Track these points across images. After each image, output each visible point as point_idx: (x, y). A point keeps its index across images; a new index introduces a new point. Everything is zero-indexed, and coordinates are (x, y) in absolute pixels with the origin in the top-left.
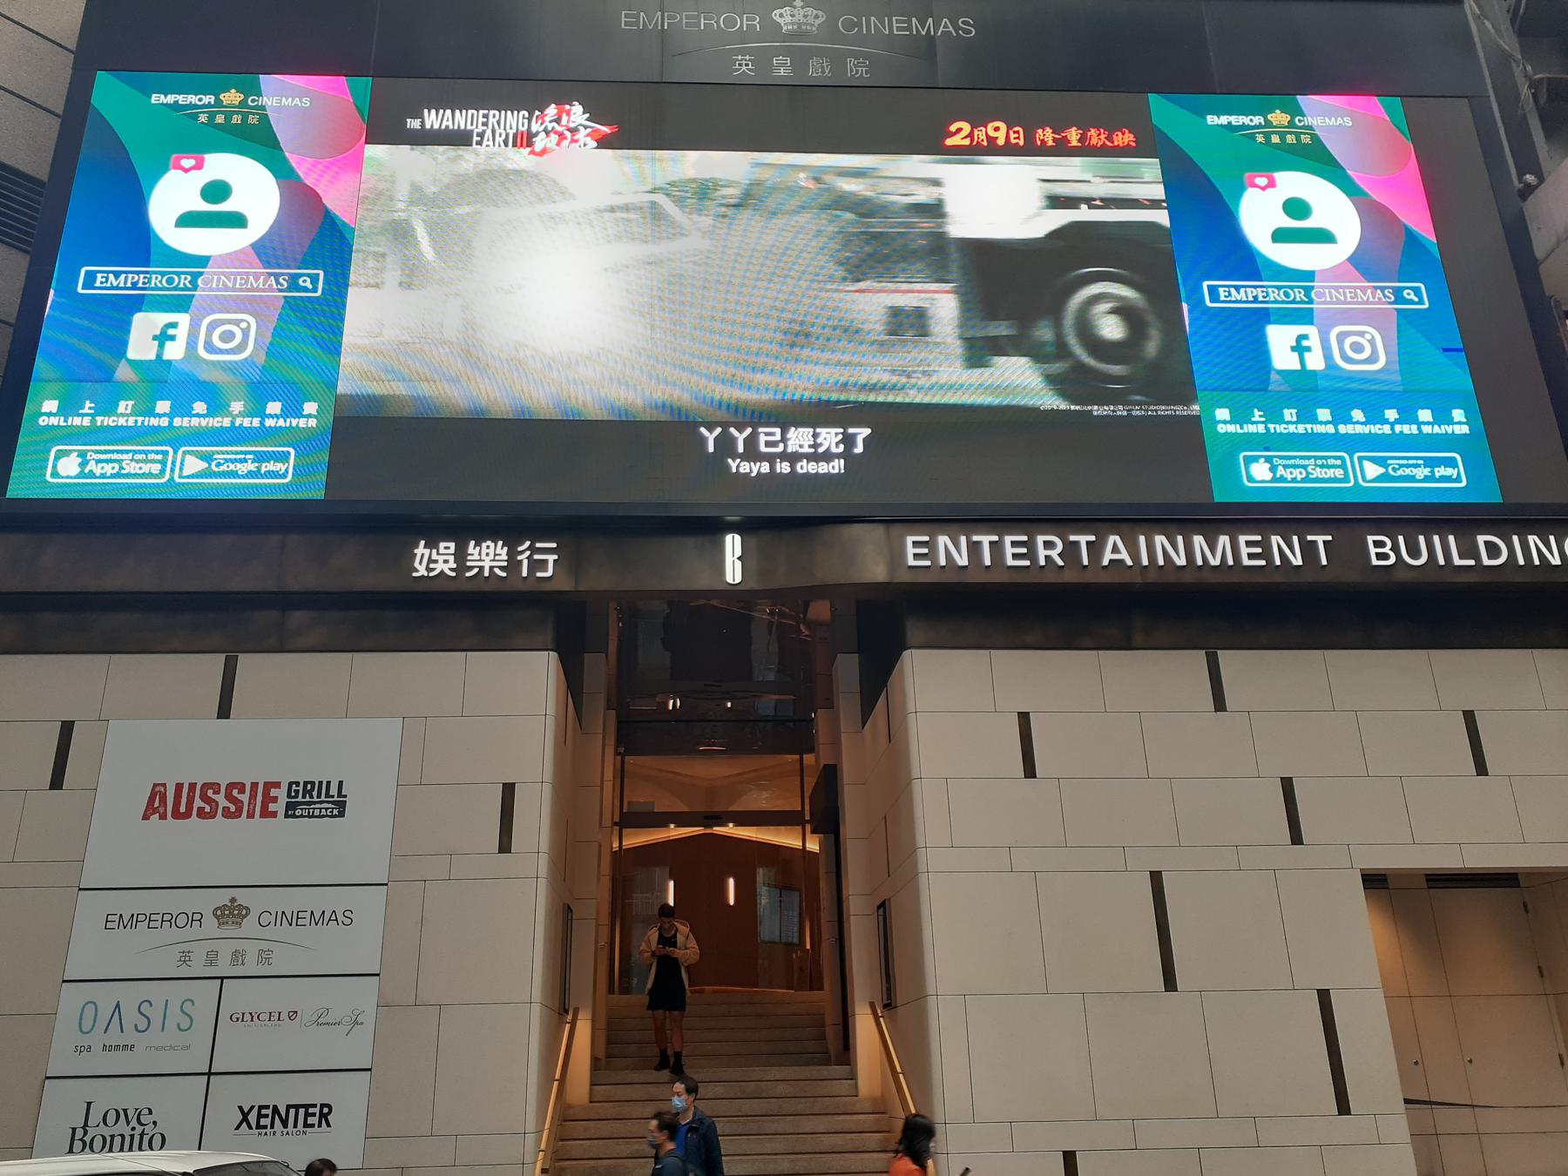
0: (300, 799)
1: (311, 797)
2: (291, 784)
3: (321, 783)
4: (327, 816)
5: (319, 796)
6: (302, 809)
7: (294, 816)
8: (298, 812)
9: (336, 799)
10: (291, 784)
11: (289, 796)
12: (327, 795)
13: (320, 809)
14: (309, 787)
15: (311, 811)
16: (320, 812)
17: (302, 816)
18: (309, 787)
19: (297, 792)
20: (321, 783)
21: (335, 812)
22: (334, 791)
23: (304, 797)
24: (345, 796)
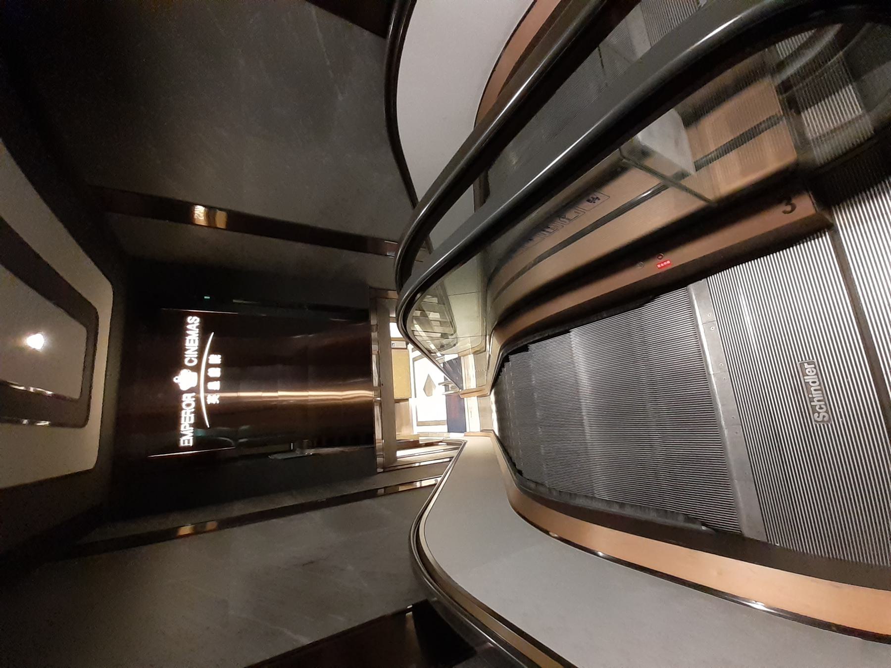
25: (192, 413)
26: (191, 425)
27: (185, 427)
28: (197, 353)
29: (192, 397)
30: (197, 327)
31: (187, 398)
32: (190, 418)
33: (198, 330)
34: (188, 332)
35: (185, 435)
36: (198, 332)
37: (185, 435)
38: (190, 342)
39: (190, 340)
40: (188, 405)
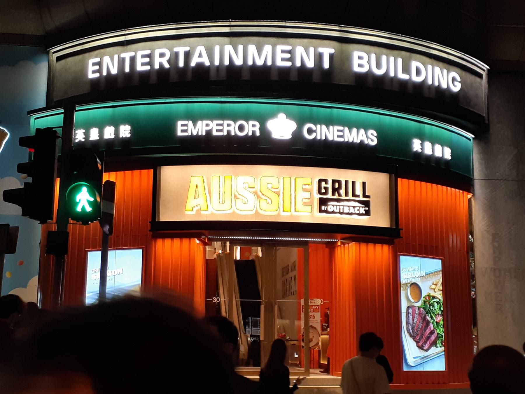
0: (329, 196)
1: (340, 195)
2: (320, 181)
3: (346, 182)
4: (355, 214)
5: (347, 194)
6: (333, 205)
7: (326, 212)
8: (330, 208)
9: (361, 198)
10: (320, 181)
11: (320, 193)
12: (354, 195)
13: (349, 206)
14: (337, 186)
15: (341, 208)
16: (349, 209)
17: (333, 212)
18: (337, 186)
19: (326, 188)
20: (346, 182)
21: (362, 211)
22: (359, 191)
23: (333, 194)
24: (369, 197)
25: (229, 132)
26: (209, 132)
27: (207, 125)
28: (324, 138)
29: (254, 132)
30: (362, 142)
31: (253, 126)
32: (221, 131)
33: (359, 141)
34: (355, 130)
35: (195, 124)
36: (355, 141)
37: (195, 124)
38: (338, 131)
39: (342, 131)
40: (241, 128)
